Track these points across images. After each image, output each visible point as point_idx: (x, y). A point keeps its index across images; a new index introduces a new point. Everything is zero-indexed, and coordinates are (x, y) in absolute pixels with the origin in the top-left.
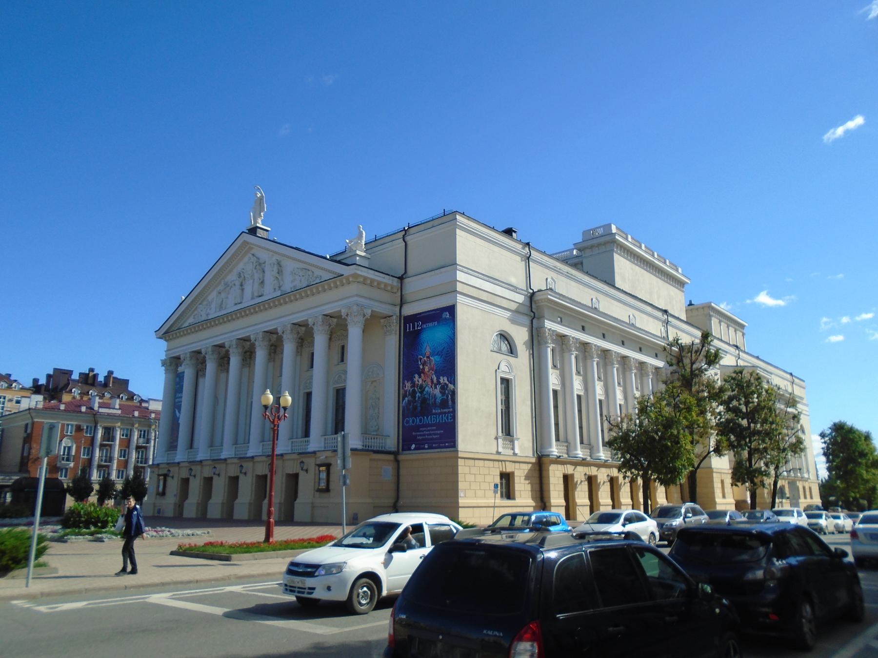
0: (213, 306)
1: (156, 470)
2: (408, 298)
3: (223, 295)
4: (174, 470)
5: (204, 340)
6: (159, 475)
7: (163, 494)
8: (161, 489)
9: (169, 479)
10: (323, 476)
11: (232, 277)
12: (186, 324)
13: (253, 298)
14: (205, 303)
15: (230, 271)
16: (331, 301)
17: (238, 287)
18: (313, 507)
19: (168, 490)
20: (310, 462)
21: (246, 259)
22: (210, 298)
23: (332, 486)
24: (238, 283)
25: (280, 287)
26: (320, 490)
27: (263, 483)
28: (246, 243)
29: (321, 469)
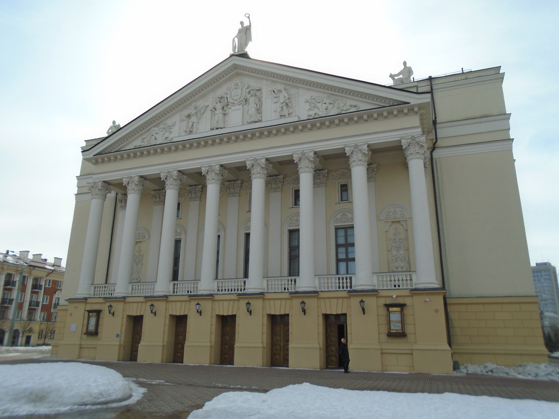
0: (175, 130)
1: (82, 308)
2: (439, 143)
3: (194, 119)
4: (118, 307)
5: (166, 166)
6: (89, 312)
7: (95, 333)
8: (92, 328)
9: (105, 317)
10: (395, 317)
11: (210, 101)
12: (131, 146)
13: (243, 125)
14: (162, 126)
15: (203, 96)
16: (384, 132)
17: (219, 111)
18: (382, 353)
19: (104, 330)
20: (370, 302)
21: (232, 84)
22: (170, 122)
23: (409, 329)
24: (219, 106)
25: (289, 114)
26: (391, 335)
27: (278, 324)
28: (235, 67)
29: (390, 309)
